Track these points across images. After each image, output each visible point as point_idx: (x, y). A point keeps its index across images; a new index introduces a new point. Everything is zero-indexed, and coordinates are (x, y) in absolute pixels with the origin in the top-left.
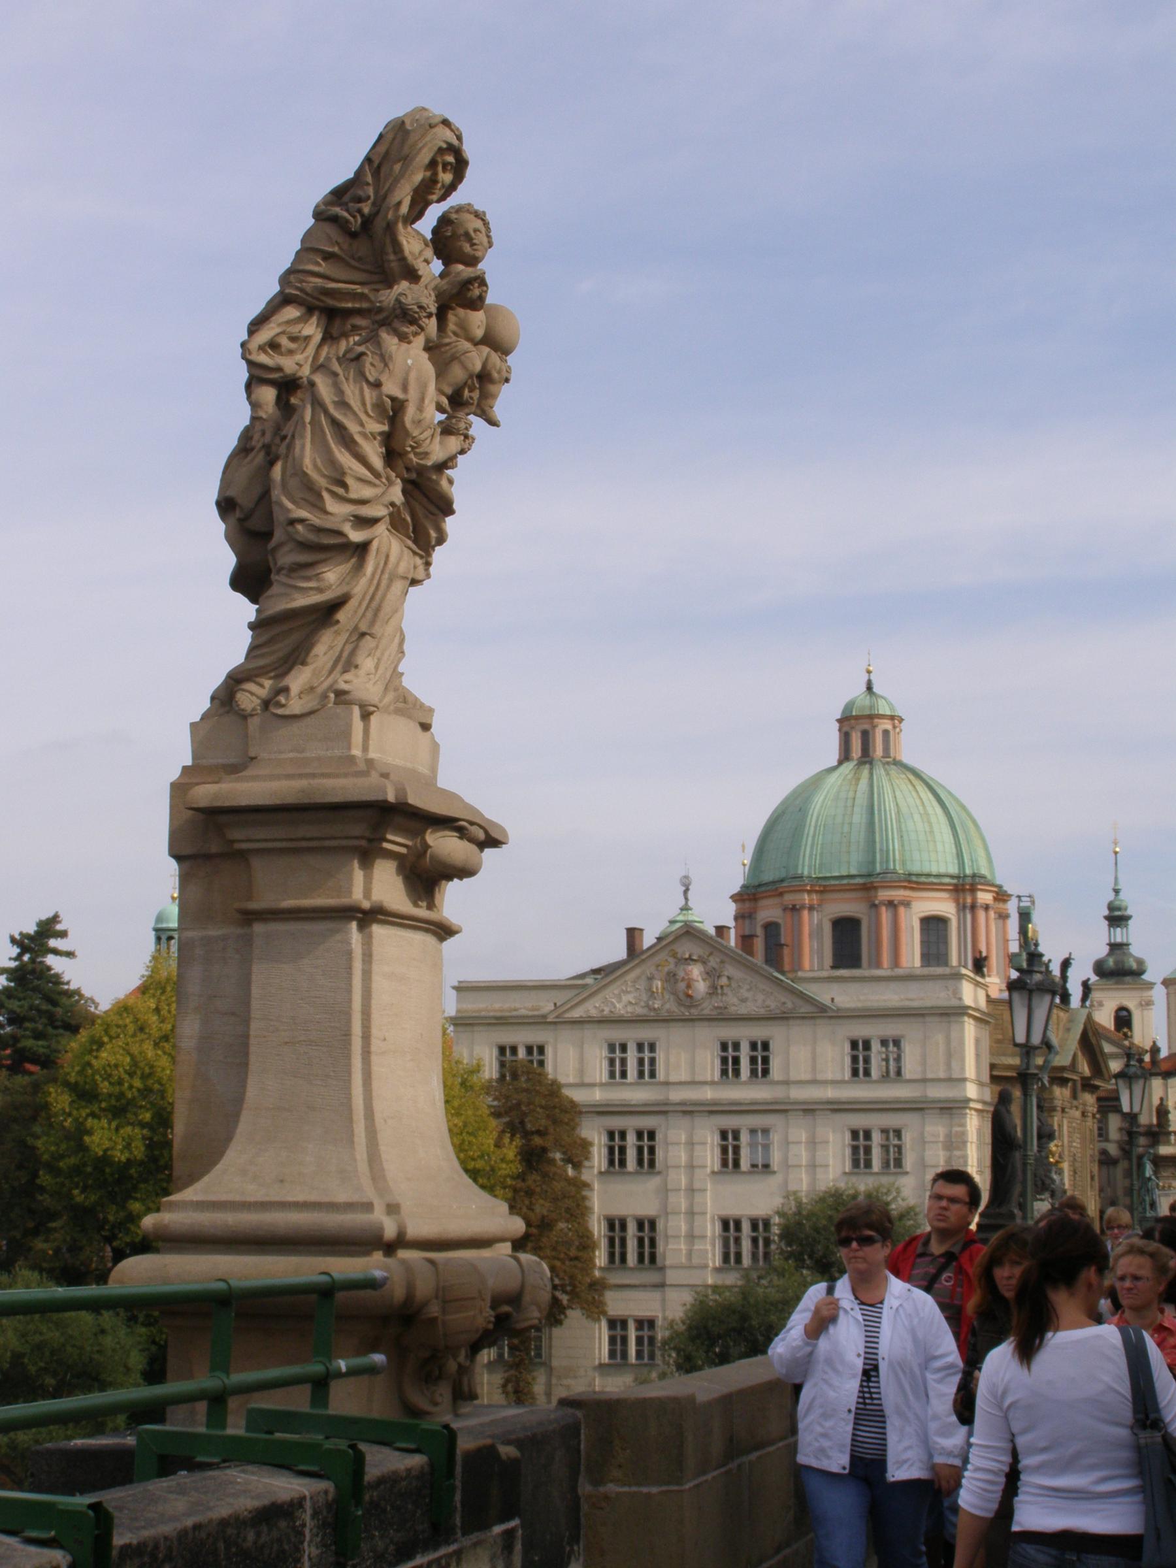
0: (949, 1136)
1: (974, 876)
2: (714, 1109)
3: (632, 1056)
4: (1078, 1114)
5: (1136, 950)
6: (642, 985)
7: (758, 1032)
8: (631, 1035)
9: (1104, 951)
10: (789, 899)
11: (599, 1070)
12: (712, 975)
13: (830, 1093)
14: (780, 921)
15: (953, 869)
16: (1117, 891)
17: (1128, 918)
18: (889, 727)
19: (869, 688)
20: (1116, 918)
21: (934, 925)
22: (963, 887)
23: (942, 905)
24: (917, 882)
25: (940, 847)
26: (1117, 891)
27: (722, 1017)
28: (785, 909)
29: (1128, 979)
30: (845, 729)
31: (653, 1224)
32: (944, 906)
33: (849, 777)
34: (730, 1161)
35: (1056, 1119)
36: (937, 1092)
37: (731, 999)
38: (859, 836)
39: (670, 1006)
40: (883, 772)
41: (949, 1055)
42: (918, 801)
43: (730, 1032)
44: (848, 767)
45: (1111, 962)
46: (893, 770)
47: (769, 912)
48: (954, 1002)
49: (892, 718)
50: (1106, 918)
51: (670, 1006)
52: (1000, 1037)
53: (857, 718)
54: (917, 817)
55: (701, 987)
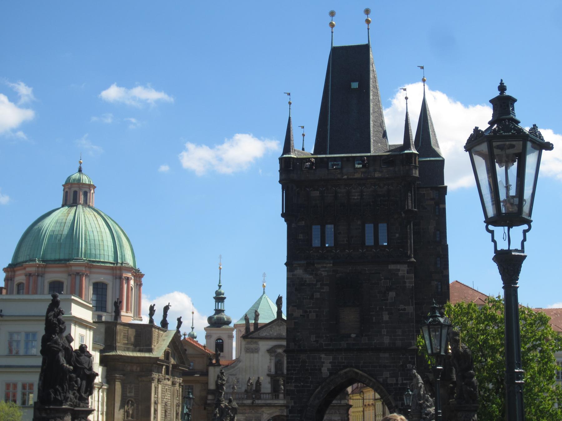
4: (170, 383)
9: (214, 312)
14: (24, 282)
15: (111, 260)
16: (220, 286)
17: (225, 298)
18: (87, 190)
20: (219, 298)
25: (106, 248)
26: (220, 286)
28: (26, 275)
30: (66, 190)
33: (65, 212)
35: (153, 385)
40: (81, 210)
42: (97, 226)
50: (214, 298)
52: (126, 342)
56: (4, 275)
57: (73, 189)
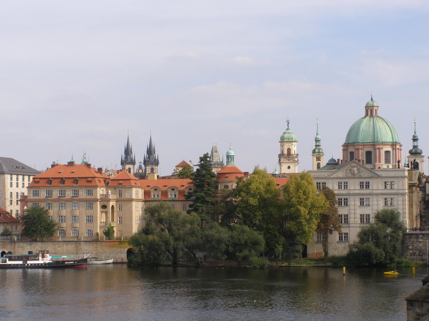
0: (403, 199)
1: (396, 142)
2: (359, 194)
3: (343, 184)
5: (420, 148)
6: (345, 171)
7: (367, 180)
8: (343, 181)
10: (356, 147)
11: (336, 187)
12: (358, 170)
13: (381, 192)
15: (391, 141)
16: (415, 133)
19: (372, 100)
20: (415, 139)
21: (387, 153)
22: (394, 145)
23: (389, 149)
24: (384, 144)
26: (415, 133)
27: (360, 177)
29: (418, 155)
31: (347, 216)
32: (389, 149)
34: (362, 204)
36: (401, 192)
37: (362, 174)
38: (371, 133)
39: (350, 175)
41: (403, 185)
43: (362, 180)
44: (368, 118)
45: (414, 151)
46: (378, 118)
47: (351, 149)
48: (404, 175)
49: (377, 106)
51: (350, 175)
53: (370, 106)
54: (384, 129)
55: (356, 172)
56: (342, 148)
57: (370, 109)
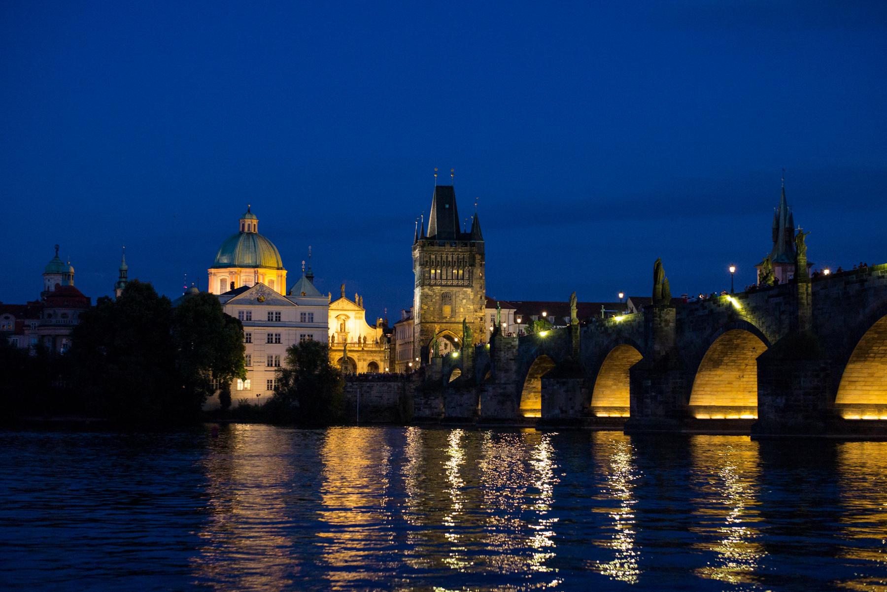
34: (270, 341)
